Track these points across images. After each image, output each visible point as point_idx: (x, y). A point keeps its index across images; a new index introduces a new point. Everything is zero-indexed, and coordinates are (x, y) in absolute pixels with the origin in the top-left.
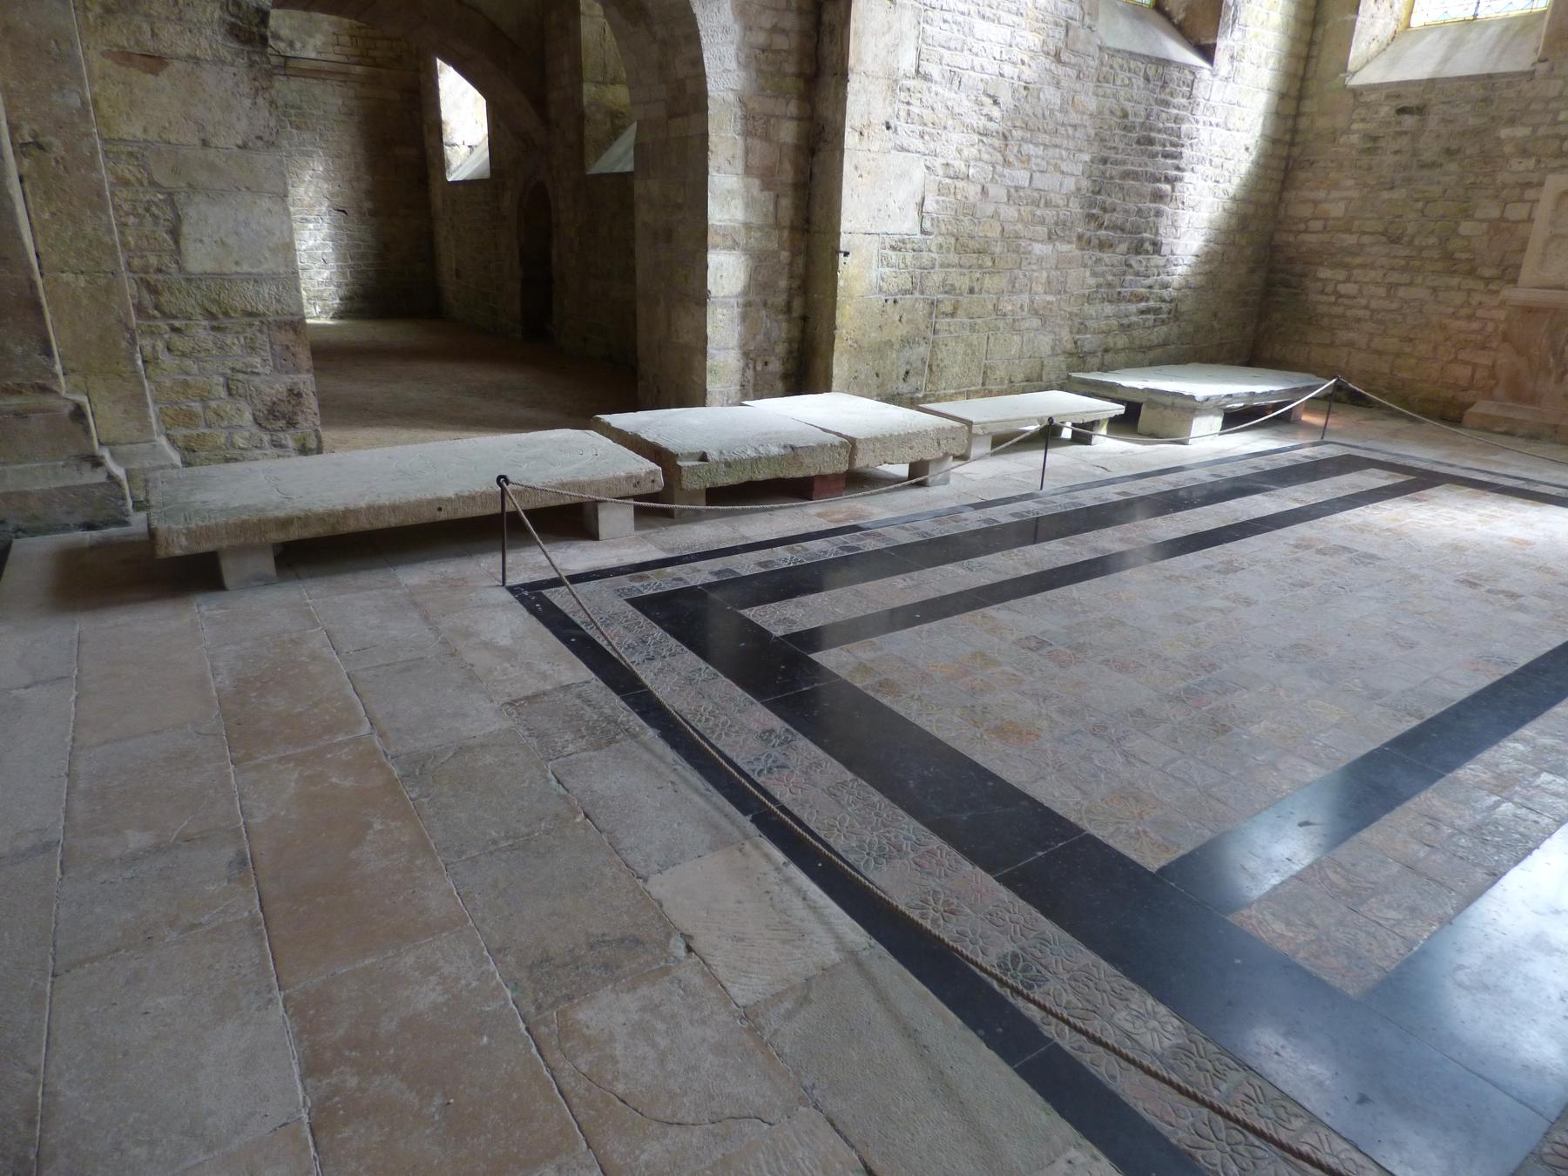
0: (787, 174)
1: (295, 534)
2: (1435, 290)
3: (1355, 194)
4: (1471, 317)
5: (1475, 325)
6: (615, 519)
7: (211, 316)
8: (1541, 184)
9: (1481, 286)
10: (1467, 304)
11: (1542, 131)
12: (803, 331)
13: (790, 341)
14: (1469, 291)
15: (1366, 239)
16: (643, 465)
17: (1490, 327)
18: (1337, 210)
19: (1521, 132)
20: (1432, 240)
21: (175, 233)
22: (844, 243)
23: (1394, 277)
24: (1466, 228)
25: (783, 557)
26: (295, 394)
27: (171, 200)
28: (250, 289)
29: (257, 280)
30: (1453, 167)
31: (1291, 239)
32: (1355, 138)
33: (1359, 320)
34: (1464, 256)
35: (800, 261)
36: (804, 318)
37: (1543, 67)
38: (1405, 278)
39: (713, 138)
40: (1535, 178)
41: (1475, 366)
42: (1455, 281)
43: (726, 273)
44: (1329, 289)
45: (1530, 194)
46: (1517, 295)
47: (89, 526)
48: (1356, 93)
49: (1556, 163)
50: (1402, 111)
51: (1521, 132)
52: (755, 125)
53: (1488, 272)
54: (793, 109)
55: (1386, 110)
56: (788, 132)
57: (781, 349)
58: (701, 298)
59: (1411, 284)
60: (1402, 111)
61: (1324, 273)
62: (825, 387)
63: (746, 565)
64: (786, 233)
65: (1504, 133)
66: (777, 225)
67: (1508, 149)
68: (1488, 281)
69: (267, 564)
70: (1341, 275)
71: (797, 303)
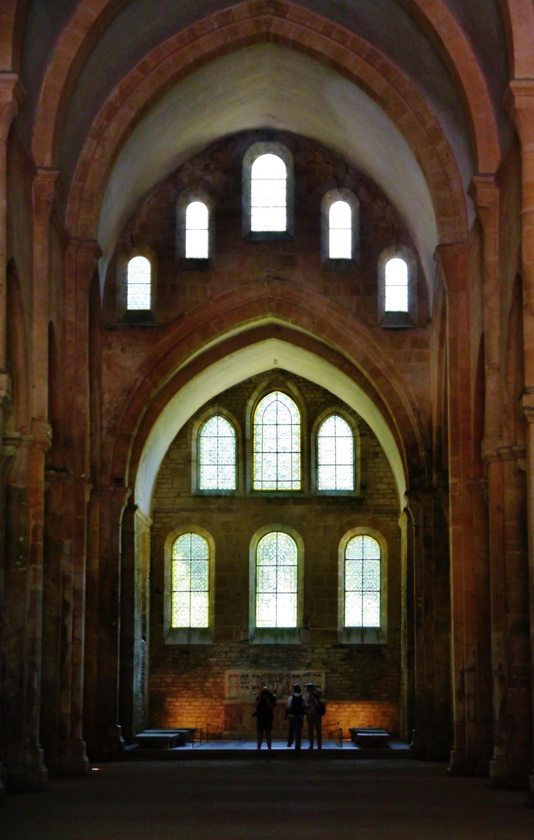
2: (202, 702)
3: (173, 675)
4: (214, 709)
5: (215, 711)
8: (223, 673)
9: (214, 700)
10: (212, 705)
11: (220, 660)
14: (212, 702)
15: (180, 689)
17: (219, 711)
18: (169, 680)
19: (215, 660)
20: (199, 688)
23: (190, 700)
24: (207, 685)
30: (200, 668)
31: (156, 689)
32: (170, 659)
33: (183, 713)
34: (208, 692)
37: (216, 644)
38: (193, 699)
40: (221, 671)
41: (218, 723)
42: (207, 699)
44: (172, 704)
45: (221, 675)
46: (226, 702)
48: (168, 646)
49: (224, 668)
50: (182, 652)
51: (215, 660)
53: (215, 696)
55: (177, 652)
59: (196, 701)
60: (182, 652)
61: (169, 699)
65: (211, 660)
67: (213, 664)
68: (216, 699)
70: (175, 700)
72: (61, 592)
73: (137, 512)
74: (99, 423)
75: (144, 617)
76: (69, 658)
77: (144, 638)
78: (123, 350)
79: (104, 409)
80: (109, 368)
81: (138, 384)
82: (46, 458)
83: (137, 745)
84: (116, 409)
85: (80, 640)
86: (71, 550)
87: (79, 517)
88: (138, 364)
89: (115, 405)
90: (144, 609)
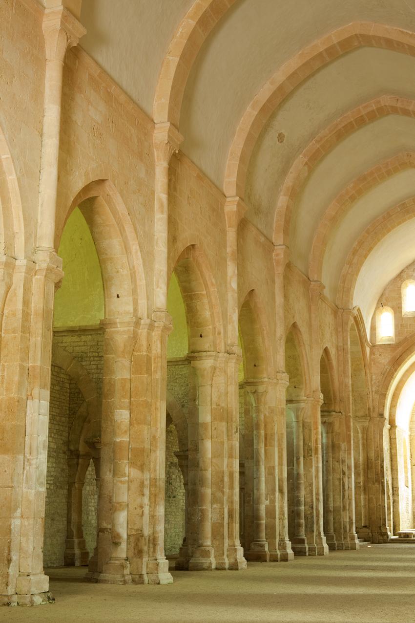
72: (341, 467)
73: (397, 428)
74: (370, 389)
75: (407, 477)
76: (346, 496)
77: (407, 487)
78: (380, 355)
79: (373, 383)
80: (374, 364)
81: (388, 370)
82: (321, 408)
83: (398, 537)
84: (378, 382)
85: (351, 488)
86: (345, 448)
87: (348, 433)
88: (388, 361)
89: (378, 380)
90: (406, 472)
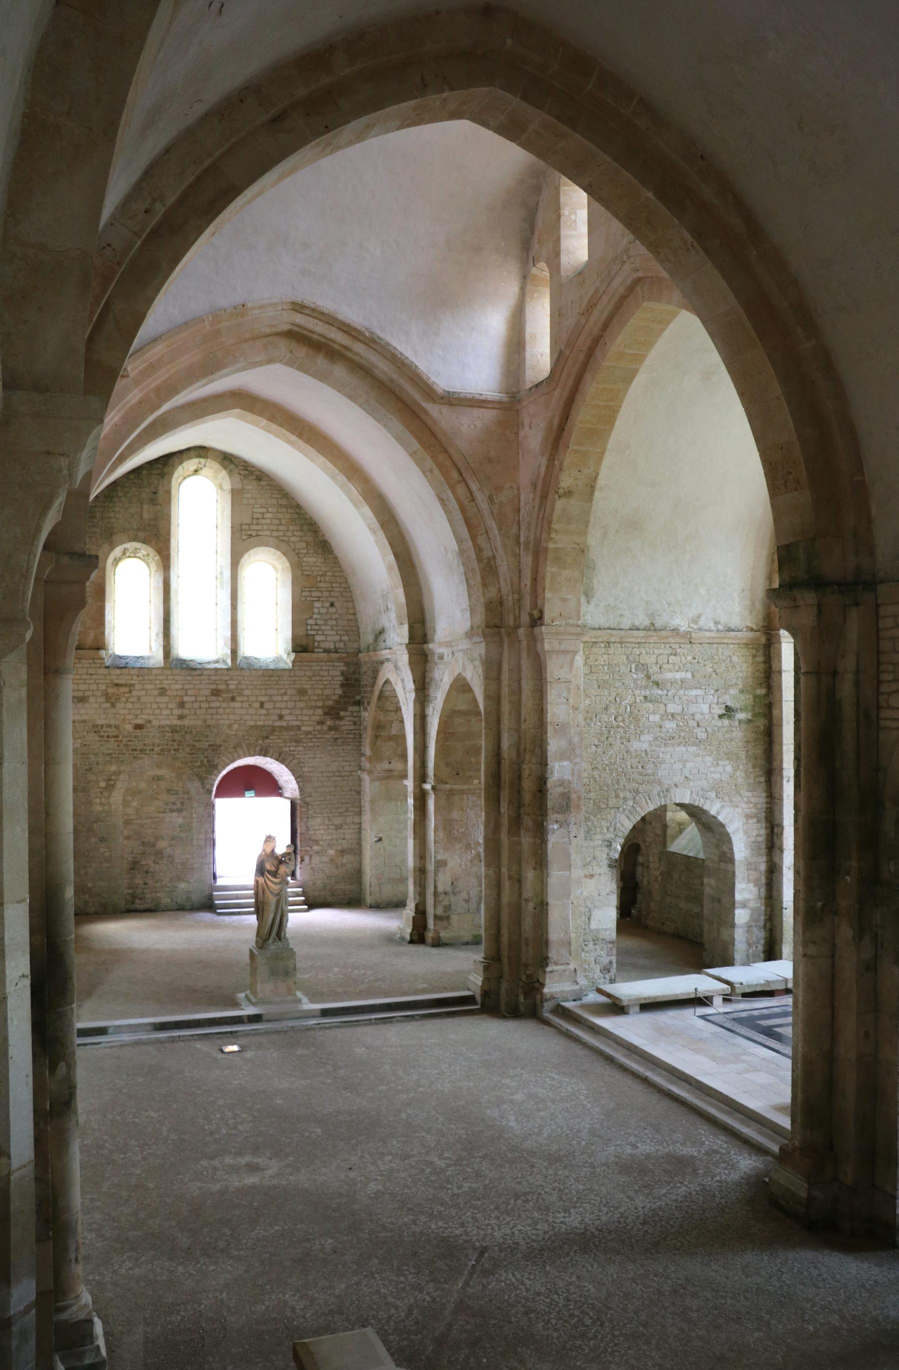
0: (763, 880)
1: (643, 1002)
6: (718, 1001)
7: (594, 940)
12: (771, 935)
13: (765, 938)
16: (725, 986)
21: (589, 919)
22: (784, 906)
25: (766, 1012)
26: (611, 962)
27: (590, 911)
28: (604, 933)
29: (606, 930)
35: (769, 909)
36: (771, 930)
39: (737, 873)
43: (741, 916)
47: (574, 1000)
52: (750, 866)
54: (764, 859)
56: (763, 867)
57: (762, 942)
58: (733, 925)
62: (781, 958)
63: (756, 1013)
64: (763, 900)
66: (760, 898)
69: (638, 1008)
71: (768, 925)
